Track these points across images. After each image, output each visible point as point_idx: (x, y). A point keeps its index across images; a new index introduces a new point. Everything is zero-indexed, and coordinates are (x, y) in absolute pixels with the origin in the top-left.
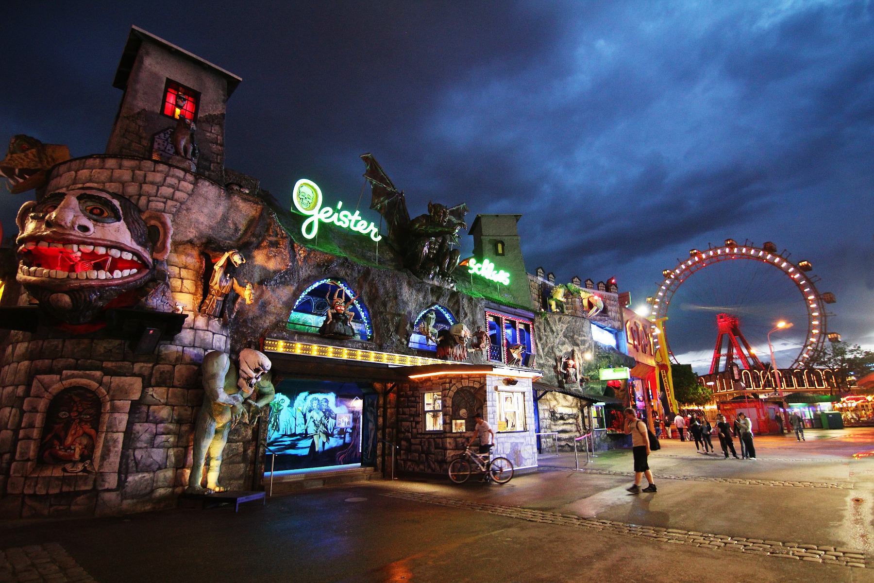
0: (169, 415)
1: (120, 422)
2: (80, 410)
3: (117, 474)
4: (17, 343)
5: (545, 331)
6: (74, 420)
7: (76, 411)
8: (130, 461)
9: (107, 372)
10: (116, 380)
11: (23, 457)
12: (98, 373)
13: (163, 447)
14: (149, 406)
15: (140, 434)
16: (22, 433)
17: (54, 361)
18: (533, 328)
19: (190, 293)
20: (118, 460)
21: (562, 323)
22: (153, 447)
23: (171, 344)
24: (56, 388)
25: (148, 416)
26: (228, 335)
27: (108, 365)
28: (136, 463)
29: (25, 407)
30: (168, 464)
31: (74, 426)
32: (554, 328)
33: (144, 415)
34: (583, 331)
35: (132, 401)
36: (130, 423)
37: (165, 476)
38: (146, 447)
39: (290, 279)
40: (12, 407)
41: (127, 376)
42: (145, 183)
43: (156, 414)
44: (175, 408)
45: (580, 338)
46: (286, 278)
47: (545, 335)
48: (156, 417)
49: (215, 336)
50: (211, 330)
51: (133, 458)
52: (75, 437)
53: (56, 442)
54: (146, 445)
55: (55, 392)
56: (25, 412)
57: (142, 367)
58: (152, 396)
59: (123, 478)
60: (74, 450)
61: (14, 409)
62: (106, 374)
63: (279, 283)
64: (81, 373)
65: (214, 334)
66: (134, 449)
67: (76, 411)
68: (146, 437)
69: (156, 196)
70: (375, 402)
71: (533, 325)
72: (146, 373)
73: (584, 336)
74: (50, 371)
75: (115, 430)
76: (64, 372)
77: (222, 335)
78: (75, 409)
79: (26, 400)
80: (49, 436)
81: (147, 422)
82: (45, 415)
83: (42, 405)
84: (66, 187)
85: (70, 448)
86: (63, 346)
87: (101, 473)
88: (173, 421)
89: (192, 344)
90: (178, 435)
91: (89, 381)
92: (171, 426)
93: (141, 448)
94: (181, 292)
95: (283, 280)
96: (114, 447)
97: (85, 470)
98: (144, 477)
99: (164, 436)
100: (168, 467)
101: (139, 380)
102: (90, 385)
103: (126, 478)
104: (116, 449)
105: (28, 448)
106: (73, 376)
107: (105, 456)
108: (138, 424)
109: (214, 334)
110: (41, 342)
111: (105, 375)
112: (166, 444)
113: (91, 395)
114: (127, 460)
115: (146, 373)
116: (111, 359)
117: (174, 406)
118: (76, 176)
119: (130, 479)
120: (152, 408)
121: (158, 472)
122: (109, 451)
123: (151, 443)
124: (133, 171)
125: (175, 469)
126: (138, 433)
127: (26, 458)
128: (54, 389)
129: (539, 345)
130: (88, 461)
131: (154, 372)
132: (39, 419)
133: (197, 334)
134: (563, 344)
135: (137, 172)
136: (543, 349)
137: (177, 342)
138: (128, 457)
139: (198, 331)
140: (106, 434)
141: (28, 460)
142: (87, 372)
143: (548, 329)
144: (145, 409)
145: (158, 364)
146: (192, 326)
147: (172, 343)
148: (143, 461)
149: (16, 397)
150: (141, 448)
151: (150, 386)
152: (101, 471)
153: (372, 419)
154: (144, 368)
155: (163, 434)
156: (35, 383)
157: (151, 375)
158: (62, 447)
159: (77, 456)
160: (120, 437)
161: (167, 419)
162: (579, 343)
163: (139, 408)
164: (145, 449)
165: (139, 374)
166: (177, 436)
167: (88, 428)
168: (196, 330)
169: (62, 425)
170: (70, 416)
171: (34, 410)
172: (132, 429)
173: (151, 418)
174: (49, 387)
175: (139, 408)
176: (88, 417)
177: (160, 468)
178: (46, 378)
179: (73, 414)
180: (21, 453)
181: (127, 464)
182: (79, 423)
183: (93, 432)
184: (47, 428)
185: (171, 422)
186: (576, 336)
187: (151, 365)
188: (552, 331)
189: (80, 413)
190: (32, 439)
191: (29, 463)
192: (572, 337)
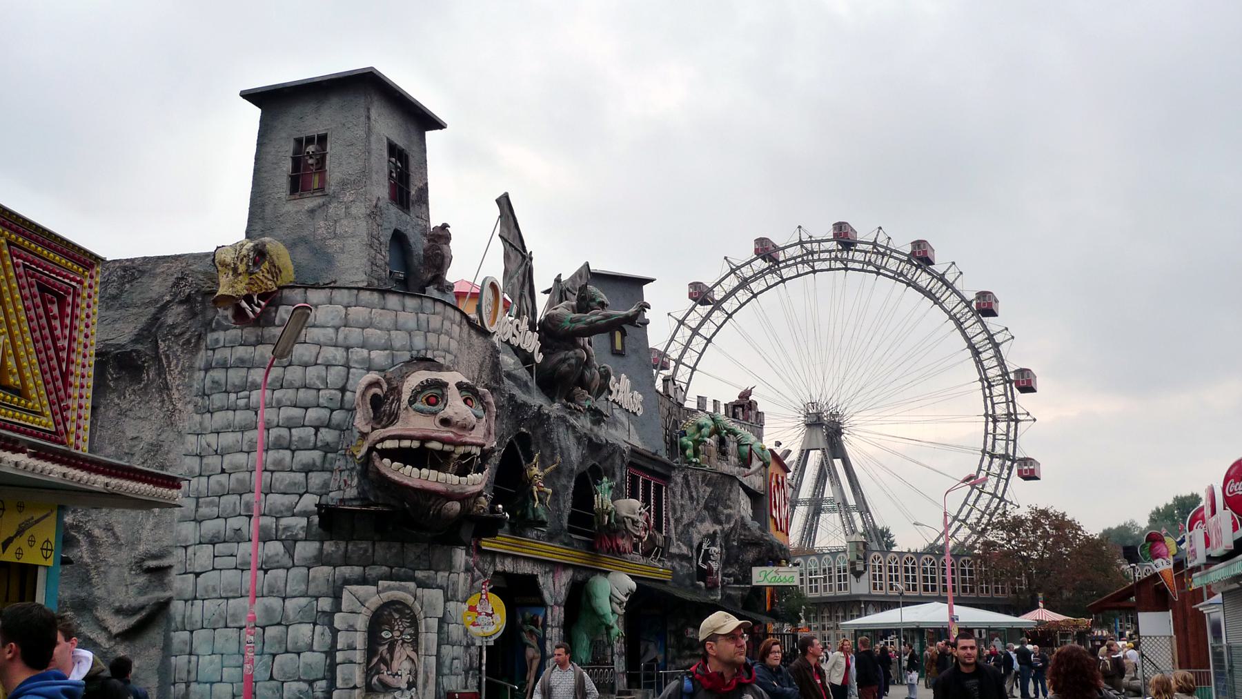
2: (401, 629)
4: (296, 541)
5: (682, 497)
6: (397, 641)
7: (398, 630)
9: (422, 584)
11: (347, 684)
16: (340, 657)
17: (367, 569)
18: (666, 492)
21: (706, 485)
24: (374, 601)
27: (419, 574)
29: (337, 625)
31: (397, 649)
32: (694, 494)
34: (729, 499)
36: (439, 645)
40: (315, 624)
42: (429, 332)
45: (725, 511)
47: (682, 506)
52: (400, 661)
53: (382, 666)
55: (373, 608)
56: (339, 631)
60: (401, 675)
61: (317, 628)
64: (397, 584)
67: (398, 630)
69: (438, 350)
70: (540, 619)
71: (666, 487)
72: (445, 586)
73: (731, 508)
74: (363, 581)
76: (380, 582)
78: (396, 628)
79: (337, 616)
80: (375, 660)
82: (366, 634)
83: (361, 622)
84: (333, 327)
85: (397, 674)
86: (374, 551)
91: (405, 594)
101: (441, 591)
105: (352, 674)
106: (389, 588)
107: (425, 686)
110: (342, 545)
111: (418, 587)
113: (409, 612)
118: (346, 315)
122: (428, 677)
124: (417, 313)
127: (352, 686)
128: (372, 603)
129: (672, 522)
130: (414, 689)
132: (360, 640)
134: (702, 521)
135: (420, 315)
136: (676, 528)
141: (355, 687)
142: (403, 583)
143: (686, 495)
144: (446, 626)
149: (317, 612)
153: (534, 643)
156: (345, 595)
157: (448, 586)
158: (389, 673)
159: (404, 686)
160: (433, 659)
162: (723, 518)
167: (409, 651)
169: (386, 646)
170: (393, 637)
171: (351, 628)
174: (365, 601)
176: (409, 637)
178: (361, 590)
179: (397, 634)
180: (344, 680)
182: (402, 644)
183: (413, 655)
184: (371, 651)
186: (720, 508)
188: (691, 498)
189: (402, 633)
190: (355, 663)
191: (357, 691)
192: (715, 509)
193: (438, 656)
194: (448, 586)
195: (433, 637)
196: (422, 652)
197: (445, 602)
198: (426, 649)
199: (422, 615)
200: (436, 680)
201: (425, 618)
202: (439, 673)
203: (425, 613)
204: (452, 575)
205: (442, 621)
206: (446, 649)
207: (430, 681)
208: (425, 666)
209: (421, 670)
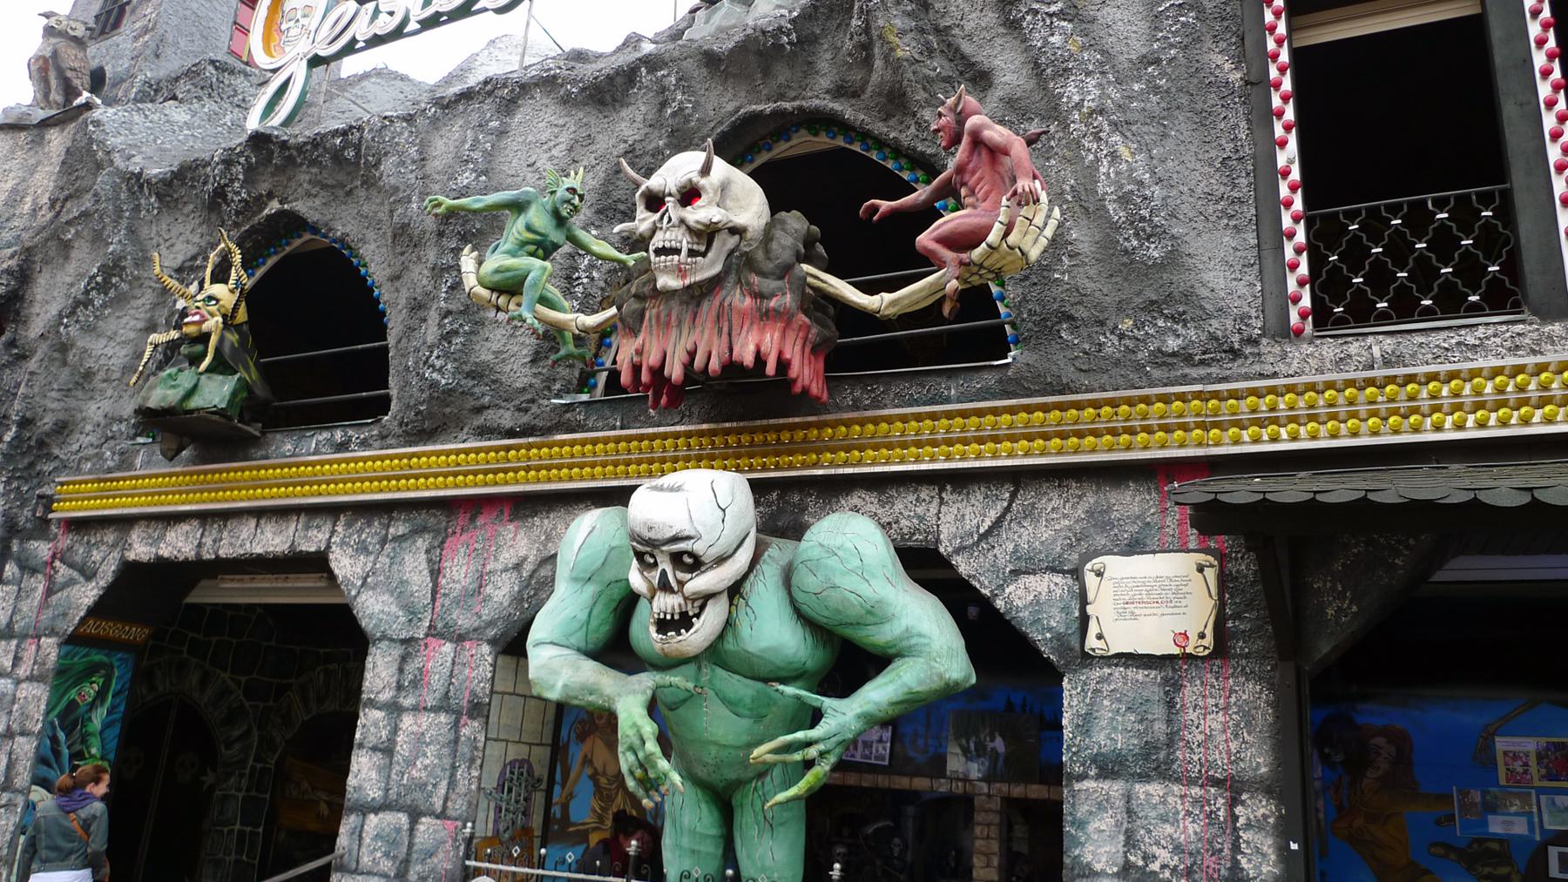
39: (130, 283)
63: (104, 306)
95: (112, 293)
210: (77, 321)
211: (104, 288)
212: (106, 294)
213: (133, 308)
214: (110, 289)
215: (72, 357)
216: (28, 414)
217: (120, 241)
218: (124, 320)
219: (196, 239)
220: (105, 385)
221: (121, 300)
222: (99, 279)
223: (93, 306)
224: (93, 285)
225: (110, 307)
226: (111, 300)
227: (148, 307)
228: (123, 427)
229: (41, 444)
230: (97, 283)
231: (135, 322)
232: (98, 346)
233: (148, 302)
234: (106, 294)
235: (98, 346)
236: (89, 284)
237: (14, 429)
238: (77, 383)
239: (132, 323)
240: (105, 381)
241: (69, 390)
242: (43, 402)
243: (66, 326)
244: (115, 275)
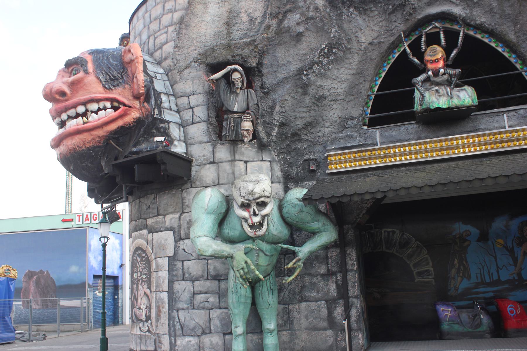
0: (203, 272)
1: (163, 282)
3: (168, 336)
8: (176, 323)
9: (152, 230)
10: (156, 235)
12: (145, 232)
13: (203, 308)
14: (183, 261)
15: (180, 293)
19: (202, 122)
20: (167, 322)
22: (194, 308)
23: (192, 187)
25: (184, 274)
26: (273, 158)
28: (181, 325)
30: (212, 328)
33: (180, 272)
35: (169, 257)
36: (171, 282)
37: (211, 342)
38: (188, 309)
39: (344, 52)
41: (161, 231)
43: (190, 270)
44: (209, 261)
46: (335, 54)
48: (190, 274)
49: (249, 164)
50: (241, 158)
51: (178, 320)
54: (186, 306)
57: (171, 219)
58: (184, 249)
59: (173, 341)
62: (149, 232)
63: (328, 64)
65: (246, 162)
66: (178, 311)
68: (186, 296)
72: (176, 226)
75: (161, 290)
77: (262, 160)
81: (183, 280)
87: (158, 334)
88: (210, 278)
89: (216, 182)
90: (219, 293)
92: (208, 284)
93: (183, 309)
94: (193, 123)
95: (332, 57)
96: (163, 308)
97: (149, 331)
98: (190, 341)
99: (203, 295)
100: (213, 331)
101: (171, 233)
102: (143, 245)
103: (175, 342)
104: (164, 310)
108: (177, 283)
109: (246, 162)
112: (206, 304)
114: (174, 322)
115: (176, 226)
116: (151, 216)
117: (207, 260)
119: (179, 342)
120: (186, 263)
121: (203, 337)
123: (191, 303)
125: (222, 335)
126: (178, 292)
131: (181, 223)
133: (220, 169)
137: (198, 183)
138: (174, 318)
139: (220, 164)
140: (156, 294)
144: (179, 265)
145: (183, 212)
146: (212, 160)
147: (193, 186)
148: (186, 323)
150: (183, 309)
151: (181, 239)
152: (157, 332)
154: (173, 220)
155: (201, 293)
157: (180, 226)
160: (165, 296)
161: (203, 276)
163: (175, 265)
164: (187, 311)
165: (171, 227)
166: (217, 296)
168: (218, 163)
172: (173, 289)
173: (187, 275)
175: (175, 265)
177: (204, 333)
181: (174, 326)
185: (208, 279)
187: (178, 215)
193: (171, 292)
194: (180, 226)
195: (164, 275)
196: (154, 289)
197: (176, 242)
198: (157, 286)
199: (153, 256)
200: (169, 314)
201: (155, 258)
202: (171, 307)
203: (156, 254)
204: (184, 215)
205: (172, 259)
206: (179, 286)
207: (162, 315)
208: (157, 302)
209: (154, 305)
210: (314, 72)
211: (326, 55)
212: (328, 58)
213: (347, 64)
214: (331, 55)
215: (311, 90)
216: (284, 121)
217: (336, 31)
218: (342, 70)
219: (376, 28)
220: (332, 103)
221: (337, 61)
222: (326, 50)
223: (322, 64)
224: (322, 54)
225: (332, 64)
226: (332, 61)
227: (356, 63)
228: (355, 122)
229: (295, 134)
230: (325, 53)
231: (349, 71)
232: (327, 84)
233: (357, 60)
234: (328, 58)
235: (327, 84)
236: (320, 53)
237: (276, 129)
238: (314, 103)
239: (347, 71)
240: (333, 100)
241: (311, 107)
242: (292, 114)
243: (306, 75)
244: (335, 48)
